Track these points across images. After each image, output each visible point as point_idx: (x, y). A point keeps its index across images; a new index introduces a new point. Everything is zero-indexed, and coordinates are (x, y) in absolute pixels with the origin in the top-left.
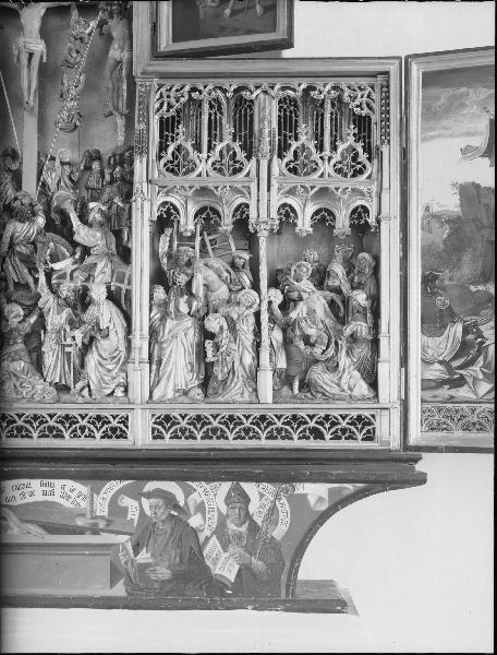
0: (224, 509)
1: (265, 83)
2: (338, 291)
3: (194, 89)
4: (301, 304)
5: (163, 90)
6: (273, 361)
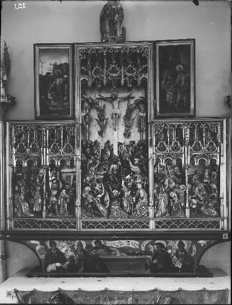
0: (177, 248)
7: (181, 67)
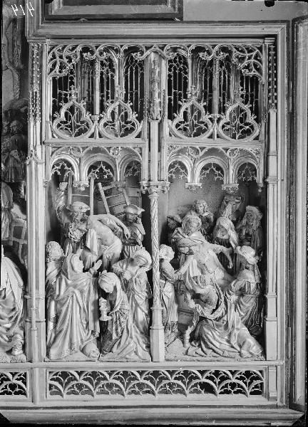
1: (156, 43)
2: (227, 244)
3: (86, 49)
4: (191, 258)
5: (55, 50)
6: (167, 311)
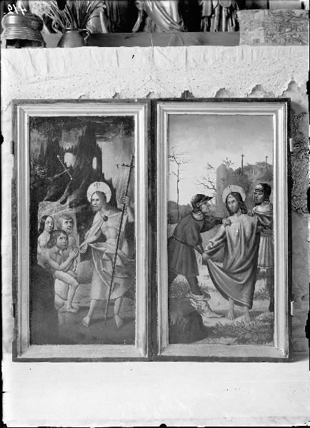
7: (104, 188)
